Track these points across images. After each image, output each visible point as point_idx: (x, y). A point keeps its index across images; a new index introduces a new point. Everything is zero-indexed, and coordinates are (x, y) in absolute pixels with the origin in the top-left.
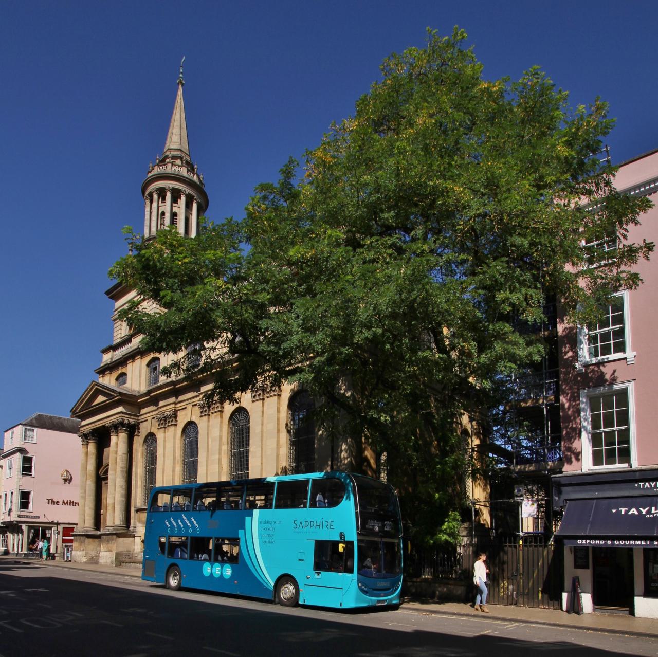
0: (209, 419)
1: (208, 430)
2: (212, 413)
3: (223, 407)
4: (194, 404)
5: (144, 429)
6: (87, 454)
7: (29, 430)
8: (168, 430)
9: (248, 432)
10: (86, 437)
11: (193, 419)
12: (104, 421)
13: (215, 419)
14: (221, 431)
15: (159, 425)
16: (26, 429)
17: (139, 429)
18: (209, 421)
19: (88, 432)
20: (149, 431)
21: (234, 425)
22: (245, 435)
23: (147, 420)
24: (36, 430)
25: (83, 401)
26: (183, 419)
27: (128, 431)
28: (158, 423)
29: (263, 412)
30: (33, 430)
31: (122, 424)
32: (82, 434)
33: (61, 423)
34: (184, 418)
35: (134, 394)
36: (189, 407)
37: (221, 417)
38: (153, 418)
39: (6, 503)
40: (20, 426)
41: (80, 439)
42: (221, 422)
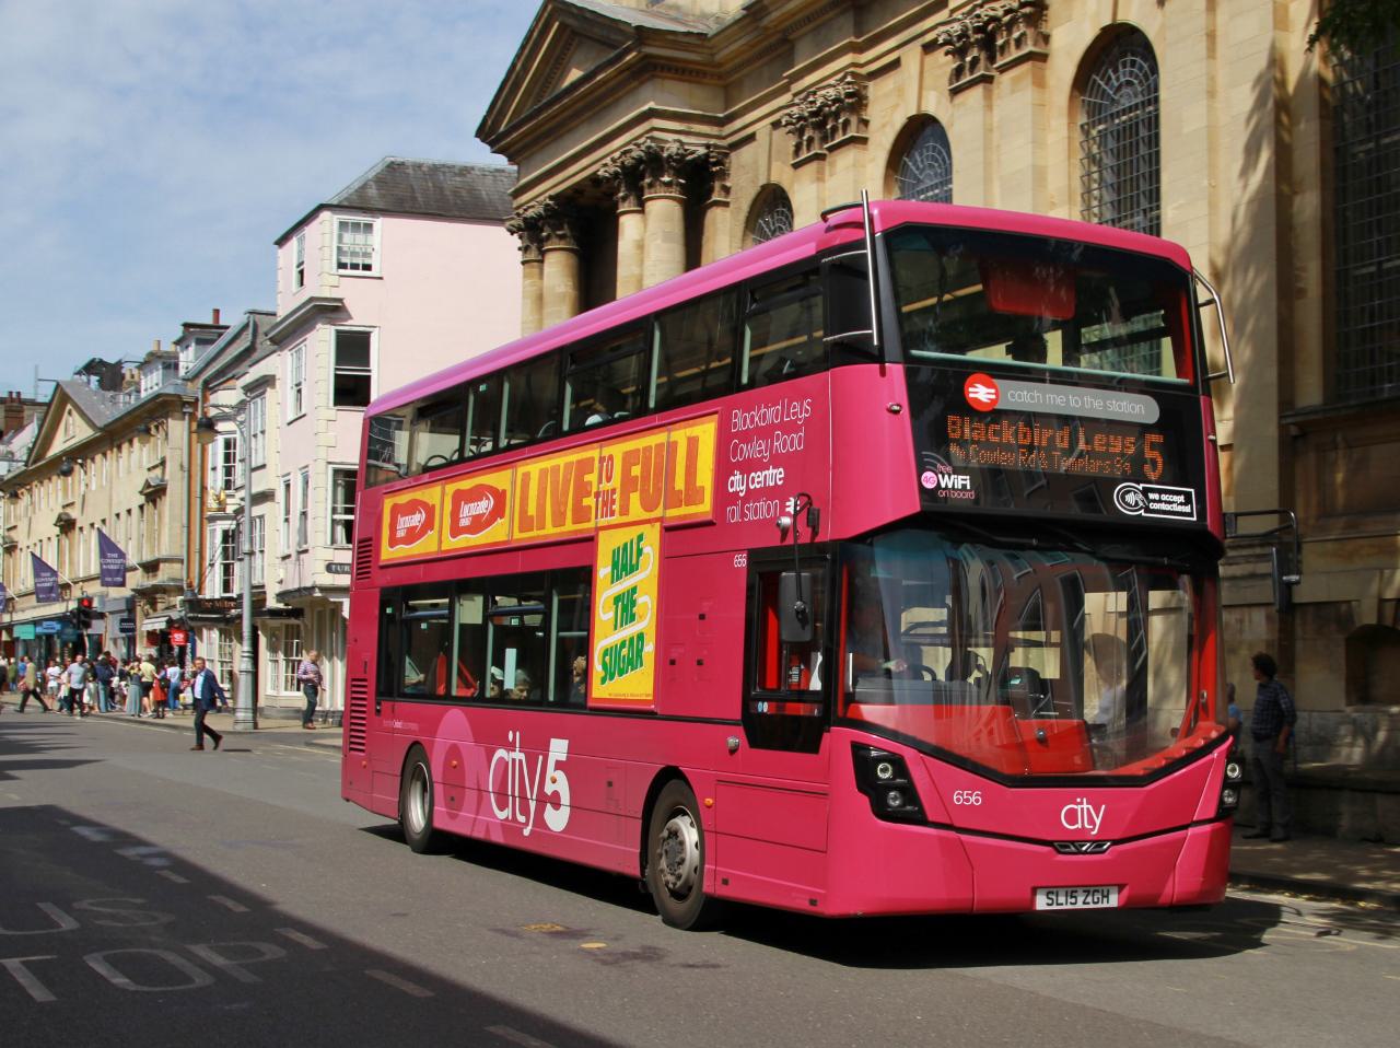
0: (988, 96)
1: (987, 147)
2: (1003, 69)
3: (1046, 38)
4: (929, 37)
5: (746, 174)
6: (540, 299)
7: (356, 226)
8: (832, 165)
9: (1154, 140)
10: (533, 233)
11: (930, 107)
12: (585, 162)
13: (1015, 94)
14: (1038, 143)
15: (797, 152)
16: (343, 225)
17: (723, 174)
18: (989, 107)
19: (541, 210)
20: (762, 181)
21: (1095, 112)
22: (1143, 150)
23: (751, 138)
24: (379, 223)
25: (516, 86)
26: (887, 112)
27: (684, 189)
28: (792, 141)
29: (1211, 36)
30: (369, 227)
31: (653, 163)
32: (518, 222)
33: (472, 190)
34: (897, 105)
35: (700, 28)
36: (910, 58)
37: (1040, 83)
38: (776, 125)
39: (287, 520)
40: (325, 215)
41: (516, 241)
42: (1040, 106)
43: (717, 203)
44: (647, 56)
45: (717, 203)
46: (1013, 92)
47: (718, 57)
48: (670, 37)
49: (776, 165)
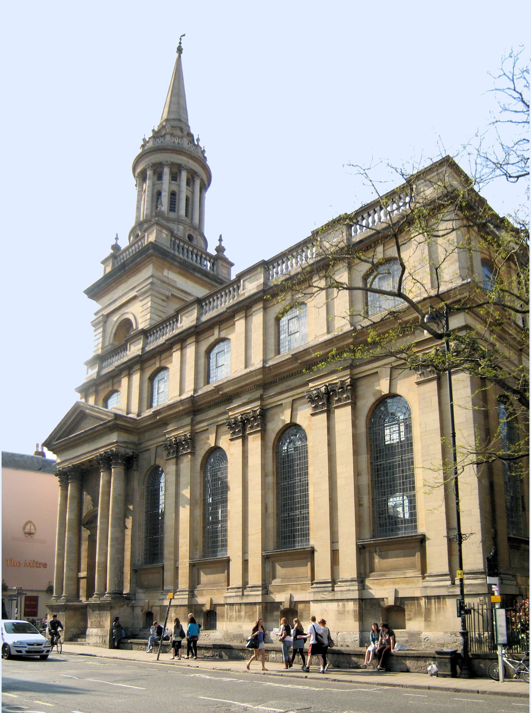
15: (169, 453)
17: (137, 460)
20: (153, 463)
43: (134, 470)
44: (116, 424)
45: (134, 470)
46: (253, 441)
47: (138, 427)
48: (125, 418)
49: (158, 459)
